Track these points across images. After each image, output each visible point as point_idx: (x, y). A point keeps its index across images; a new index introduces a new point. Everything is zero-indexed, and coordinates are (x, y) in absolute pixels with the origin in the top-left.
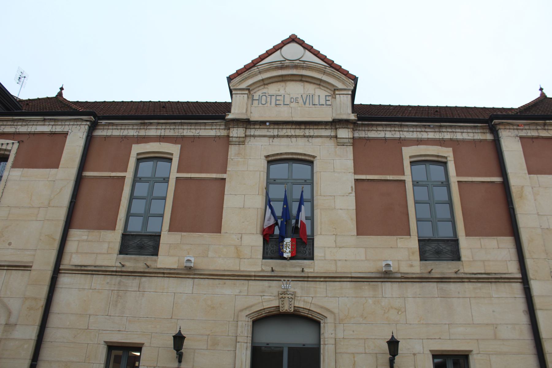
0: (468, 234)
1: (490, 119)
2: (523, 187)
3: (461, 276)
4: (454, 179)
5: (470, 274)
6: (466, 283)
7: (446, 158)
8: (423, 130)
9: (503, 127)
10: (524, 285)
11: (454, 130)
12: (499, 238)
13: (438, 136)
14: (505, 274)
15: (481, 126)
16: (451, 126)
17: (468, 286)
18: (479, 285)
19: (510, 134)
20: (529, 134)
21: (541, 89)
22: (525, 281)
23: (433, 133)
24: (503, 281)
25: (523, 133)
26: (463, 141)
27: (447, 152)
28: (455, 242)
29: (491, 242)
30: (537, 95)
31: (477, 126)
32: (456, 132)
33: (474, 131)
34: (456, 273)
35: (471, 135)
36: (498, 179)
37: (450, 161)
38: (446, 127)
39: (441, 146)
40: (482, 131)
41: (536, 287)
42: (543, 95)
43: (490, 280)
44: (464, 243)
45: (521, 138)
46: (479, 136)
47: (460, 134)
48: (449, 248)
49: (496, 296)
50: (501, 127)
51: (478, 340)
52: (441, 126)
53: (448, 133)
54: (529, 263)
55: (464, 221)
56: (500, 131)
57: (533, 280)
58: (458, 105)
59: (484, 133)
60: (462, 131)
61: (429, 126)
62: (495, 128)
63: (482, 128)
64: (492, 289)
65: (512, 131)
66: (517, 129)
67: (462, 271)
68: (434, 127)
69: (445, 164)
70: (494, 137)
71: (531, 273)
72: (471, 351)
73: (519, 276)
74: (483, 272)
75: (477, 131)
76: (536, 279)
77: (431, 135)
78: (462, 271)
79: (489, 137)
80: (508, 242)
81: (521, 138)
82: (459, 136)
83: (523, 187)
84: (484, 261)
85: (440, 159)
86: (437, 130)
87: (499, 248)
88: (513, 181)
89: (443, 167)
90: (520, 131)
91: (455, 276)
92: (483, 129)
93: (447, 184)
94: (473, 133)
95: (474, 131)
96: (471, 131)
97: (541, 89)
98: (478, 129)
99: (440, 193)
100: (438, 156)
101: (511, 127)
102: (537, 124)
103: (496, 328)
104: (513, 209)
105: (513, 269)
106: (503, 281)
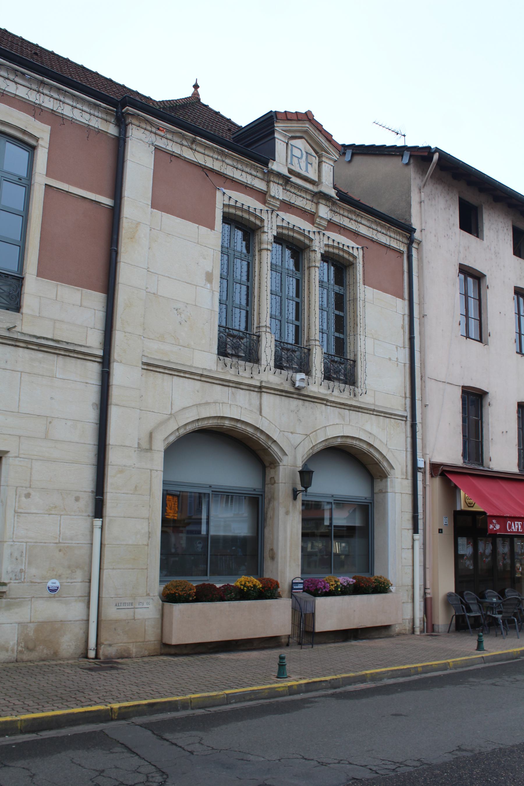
0: (40, 274)
1: (121, 103)
2: (139, 223)
3: (15, 336)
4: (40, 179)
5: (30, 336)
6: (21, 349)
7: (37, 139)
8: (12, 77)
9: (137, 123)
10: (103, 367)
11: (62, 99)
12: (85, 290)
13: (33, 97)
14: (81, 346)
15: (105, 108)
16: (59, 89)
17: (22, 353)
18: (40, 355)
19: (143, 137)
20: (169, 148)
21: (196, 86)
22: (106, 361)
23: (26, 90)
24: (76, 355)
25: (161, 143)
26: (72, 121)
27: (41, 131)
28: (19, 280)
29: (71, 294)
30: (188, 93)
31: (99, 106)
32: (64, 103)
33: (92, 112)
34: (9, 329)
35: (87, 116)
36: (107, 201)
37: (42, 146)
38: (51, 87)
39: (34, 116)
40: (104, 116)
41: (119, 374)
42: (196, 97)
43: (57, 352)
44: (33, 287)
45: (157, 149)
46: (96, 123)
47: (70, 107)
48: (5, 288)
49: (61, 376)
50: (134, 121)
51: (20, 437)
52: (42, 82)
53: (52, 99)
54: (118, 336)
55: (40, 250)
56: (130, 126)
57: (118, 362)
58: (72, 59)
59: (106, 121)
60: (74, 104)
61: (24, 74)
62: (125, 120)
63: (106, 111)
64: (59, 365)
65: (147, 133)
66: (156, 134)
67: (18, 329)
68: (31, 80)
69: (32, 149)
70: (120, 133)
71: (117, 353)
72: (7, 452)
73: (100, 353)
74: (50, 336)
75: (96, 114)
76: (121, 362)
77: (22, 92)
78: (18, 329)
79: (112, 130)
80: (97, 299)
81: (157, 149)
82: (67, 111)
83: (139, 223)
84: (55, 321)
85: (26, 138)
86: (34, 87)
87: (81, 306)
88: (129, 211)
89: (27, 153)
90: (158, 138)
91: (7, 334)
92: (107, 113)
93: (27, 182)
94: (90, 114)
95: (92, 112)
96: (88, 110)
97: (196, 86)
98: (99, 111)
99: (13, 195)
100: (24, 132)
101: (149, 128)
102: (183, 137)
103: (50, 423)
104: (117, 252)
105: (94, 342)
106: (76, 355)
